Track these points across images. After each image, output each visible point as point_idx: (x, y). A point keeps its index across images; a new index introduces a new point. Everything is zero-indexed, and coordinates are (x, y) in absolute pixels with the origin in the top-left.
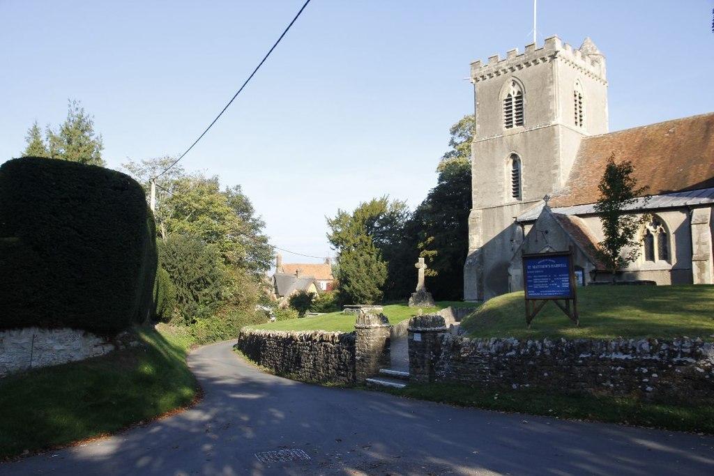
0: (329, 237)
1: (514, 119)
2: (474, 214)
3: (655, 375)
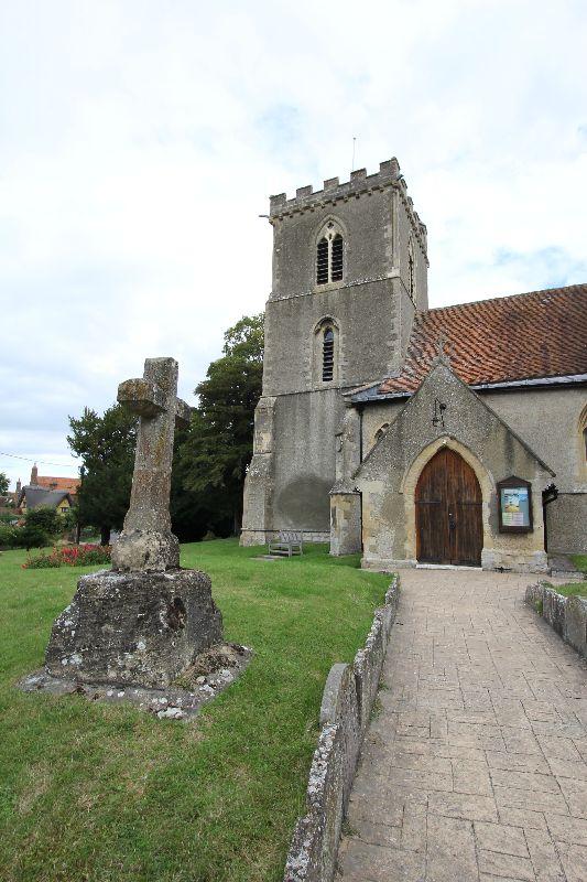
0: (69, 439)
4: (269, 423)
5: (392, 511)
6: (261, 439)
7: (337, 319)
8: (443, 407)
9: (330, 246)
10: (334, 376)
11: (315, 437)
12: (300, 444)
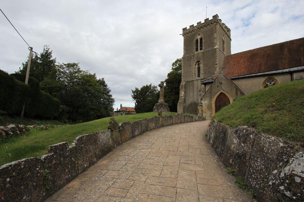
0: (132, 96)
1: (199, 48)
4: (184, 89)
5: (209, 107)
7: (201, 61)
8: (221, 83)
9: (199, 41)
11: (195, 93)
12: (191, 94)
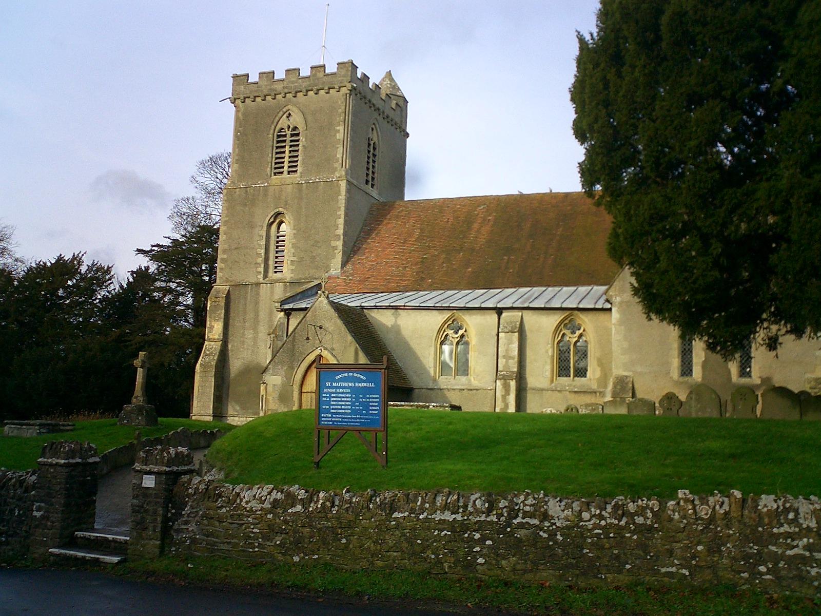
2: (218, 292)
3: (489, 542)
6: (212, 327)
10: (285, 269)
12: (249, 334)
